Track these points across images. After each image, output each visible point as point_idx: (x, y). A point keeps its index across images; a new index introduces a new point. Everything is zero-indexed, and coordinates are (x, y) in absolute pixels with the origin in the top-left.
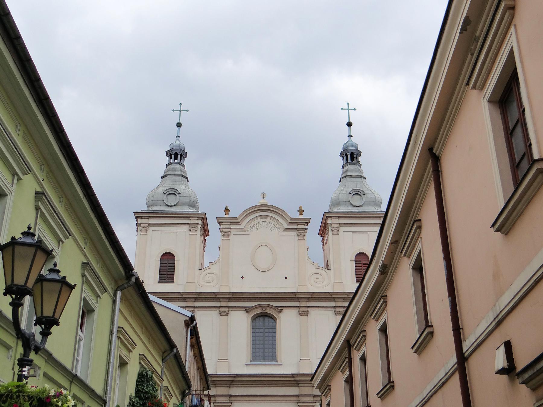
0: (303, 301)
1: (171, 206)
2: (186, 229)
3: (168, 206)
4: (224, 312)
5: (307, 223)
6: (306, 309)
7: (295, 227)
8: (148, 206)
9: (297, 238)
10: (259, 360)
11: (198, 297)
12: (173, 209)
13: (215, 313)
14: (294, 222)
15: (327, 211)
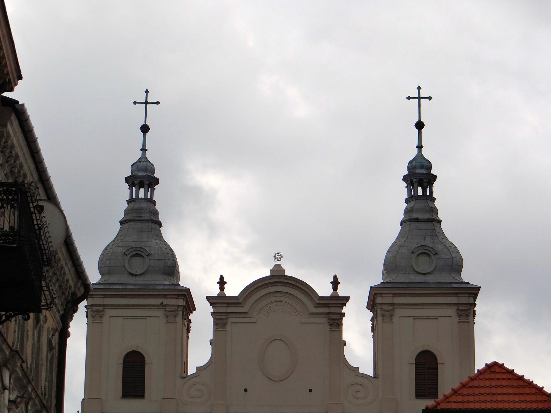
2: (160, 313)
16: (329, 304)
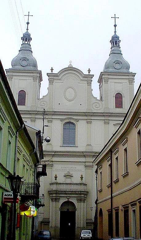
0: (89, 116)
14: (86, 76)
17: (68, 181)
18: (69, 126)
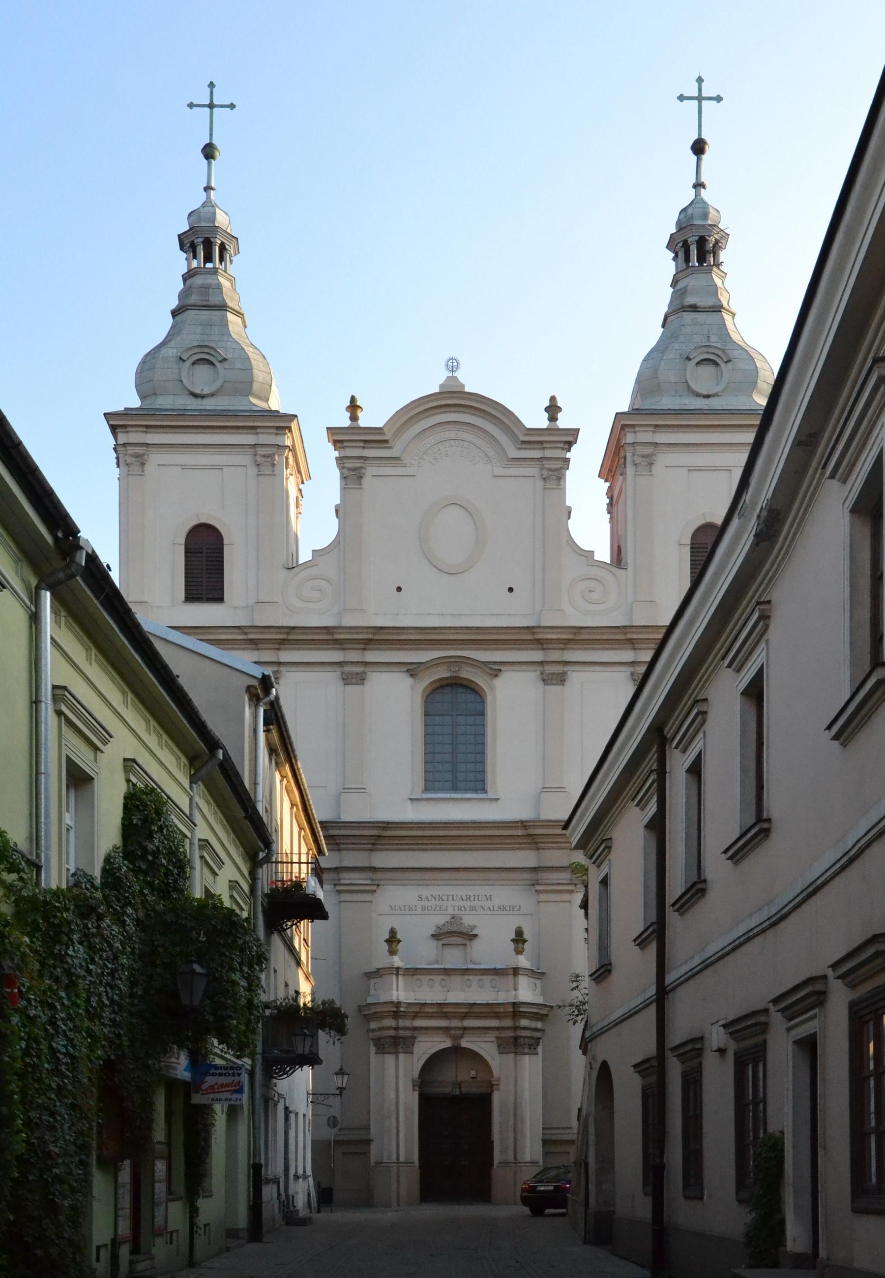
0: (552, 649)
1: (203, 397)
2: (245, 459)
3: (195, 396)
4: (354, 677)
5: (569, 444)
6: (559, 669)
7: (537, 454)
8: (143, 397)
9: (540, 484)
10: (443, 790)
11: (289, 637)
12: (209, 404)
13: (331, 677)
15: (625, 408)
16: (541, 442)
17: (453, 958)
18: (455, 707)
